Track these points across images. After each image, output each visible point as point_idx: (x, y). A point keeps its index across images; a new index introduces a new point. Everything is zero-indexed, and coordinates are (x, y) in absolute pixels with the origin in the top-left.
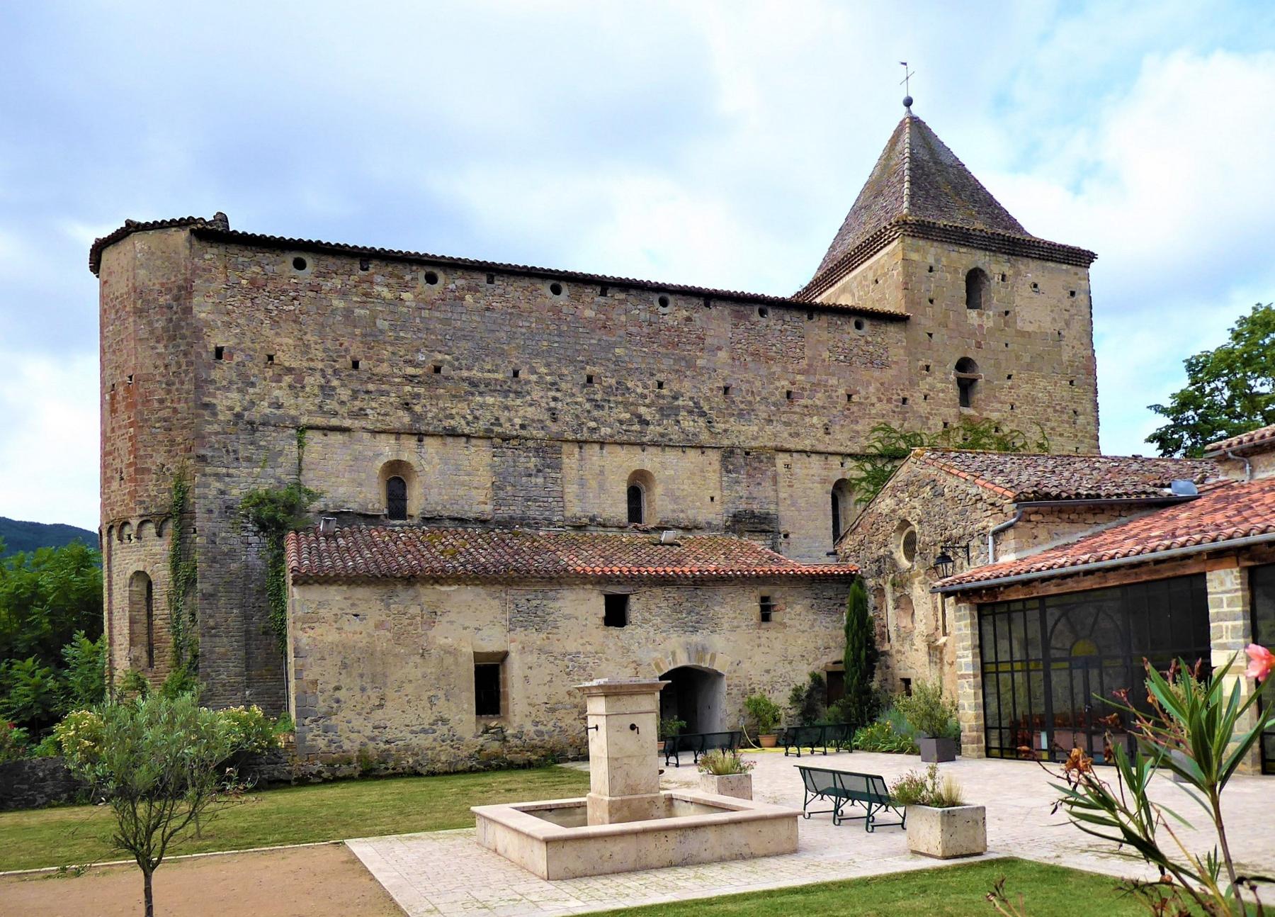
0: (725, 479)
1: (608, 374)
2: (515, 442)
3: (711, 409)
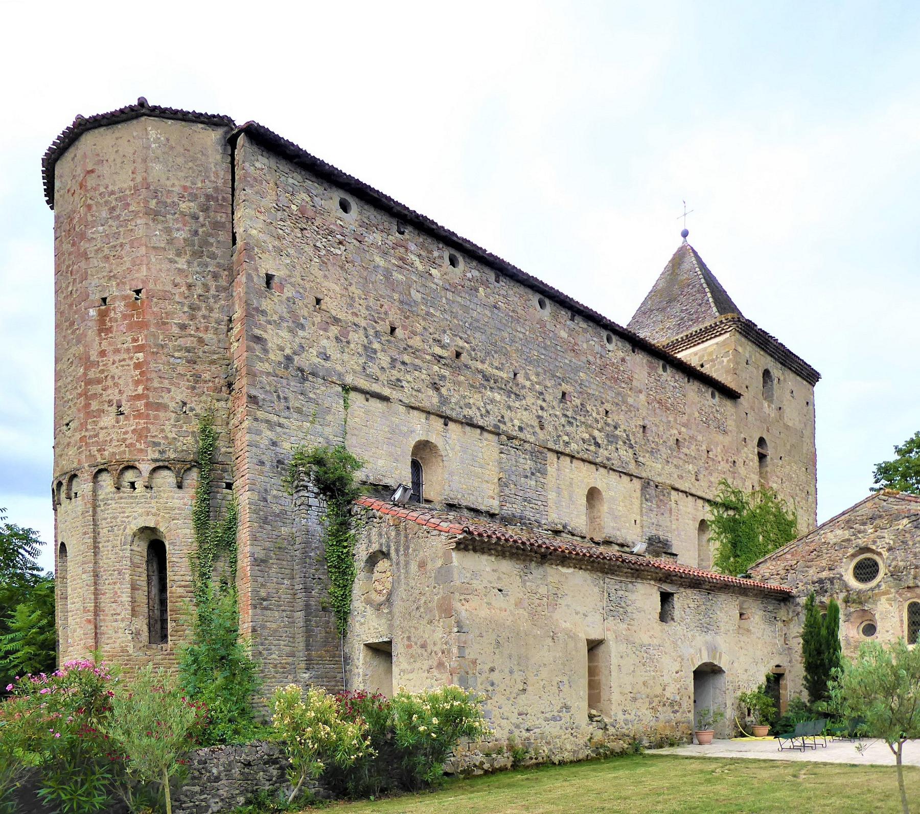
0: (645, 506)
1: (575, 394)
2: (516, 442)
3: (636, 443)
